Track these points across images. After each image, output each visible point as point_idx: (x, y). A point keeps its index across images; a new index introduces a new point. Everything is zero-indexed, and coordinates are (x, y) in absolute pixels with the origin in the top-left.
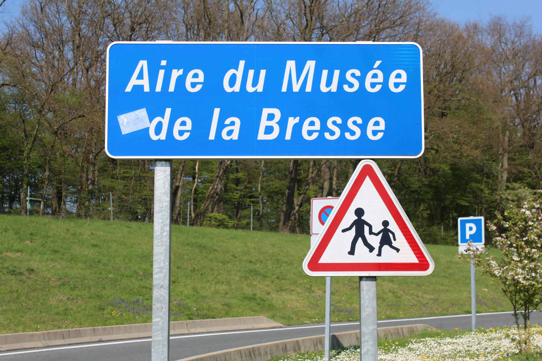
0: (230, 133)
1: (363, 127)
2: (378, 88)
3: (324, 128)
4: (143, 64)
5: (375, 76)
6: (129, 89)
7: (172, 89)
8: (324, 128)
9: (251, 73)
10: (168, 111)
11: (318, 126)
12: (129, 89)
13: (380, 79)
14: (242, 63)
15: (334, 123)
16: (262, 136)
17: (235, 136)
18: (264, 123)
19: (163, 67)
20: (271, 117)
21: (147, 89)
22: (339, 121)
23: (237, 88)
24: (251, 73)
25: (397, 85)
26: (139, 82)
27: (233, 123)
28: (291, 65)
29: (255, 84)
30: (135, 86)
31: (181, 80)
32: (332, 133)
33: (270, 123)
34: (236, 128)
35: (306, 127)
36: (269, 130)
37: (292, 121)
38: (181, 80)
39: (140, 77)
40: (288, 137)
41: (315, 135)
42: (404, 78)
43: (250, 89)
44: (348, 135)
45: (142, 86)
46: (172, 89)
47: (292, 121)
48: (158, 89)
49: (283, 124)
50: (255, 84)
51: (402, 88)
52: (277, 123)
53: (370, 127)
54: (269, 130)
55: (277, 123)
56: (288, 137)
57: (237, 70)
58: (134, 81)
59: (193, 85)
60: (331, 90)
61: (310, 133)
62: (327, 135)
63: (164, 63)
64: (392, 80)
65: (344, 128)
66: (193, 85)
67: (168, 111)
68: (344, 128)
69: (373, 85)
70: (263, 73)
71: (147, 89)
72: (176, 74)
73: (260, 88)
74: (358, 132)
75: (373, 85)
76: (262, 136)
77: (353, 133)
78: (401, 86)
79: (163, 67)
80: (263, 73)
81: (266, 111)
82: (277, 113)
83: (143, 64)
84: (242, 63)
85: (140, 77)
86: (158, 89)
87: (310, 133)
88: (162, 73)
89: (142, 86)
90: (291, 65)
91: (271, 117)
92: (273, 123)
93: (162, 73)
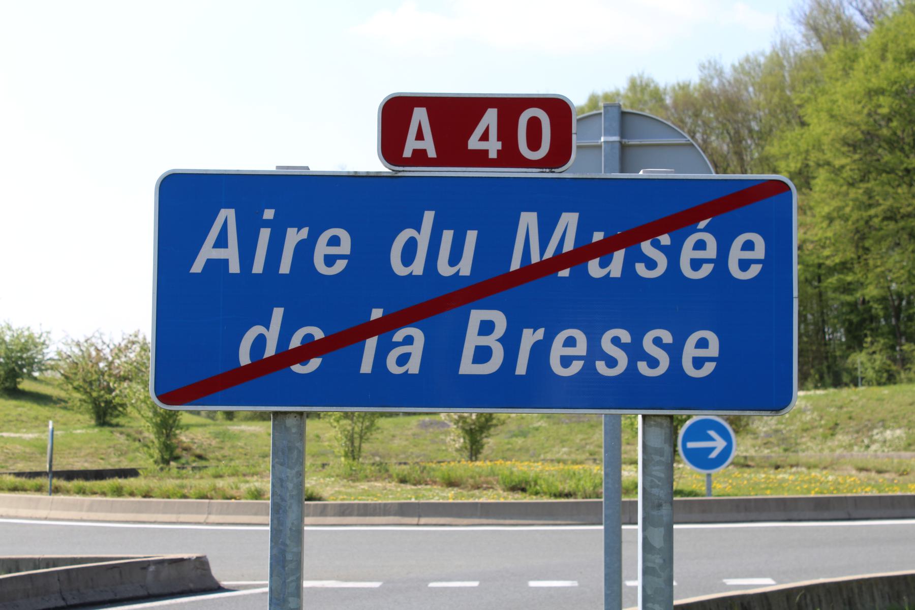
0: (403, 360)
2: (706, 270)
6: (197, 267)
7: (285, 267)
9: (448, 236)
10: (278, 314)
11: (581, 348)
12: (197, 267)
13: (711, 251)
14: (429, 217)
15: (616, 341)
17: (414, 366)
19: (267, 223)
20: (486, 328)
21: (234, 268)
22: (625, 336)
23: (418, 267)
24: (448, 236)
25: (744, 265)
26: (219, 254)
27: (409, 340)
28: (529, 221)
30: (210, 263)
32: (612, 362)
34: (417, 350)
39: (221, 242)
40: (521, 368)
41: (576, 367)
42: (759, 252)
43: (444, 269)
44: (643, 368)
45: (226, 262)
46: (285, 267)
48: (258, 267)
52: (498, 340)
53: (690, 351)
55: (498, 340)
56: (521, 368)
57: (419, 231)
59: (330, 260)
61: (566, 361)
62: (601, 367)
63: (269, 214)
64: (736, 253)
66: (330, 260)
67: (278, 314)
69: (696, 264)
70: (472, 237)
71: (234, 268)
73: (465, 267)
74: (664, 360)
75: (696, 264)
77: (653, 363)
79: (267, 223)
80: (472, 237)
81: (477, 316)
84: (429, 217)
85: (221, 242)
86: (258, 267)
87: (566, 361)
88: (265, 235)
89: (226, 262)
90: (529, 221)
91: (486, 328)
92: (491, 341)
93: (265, 235)
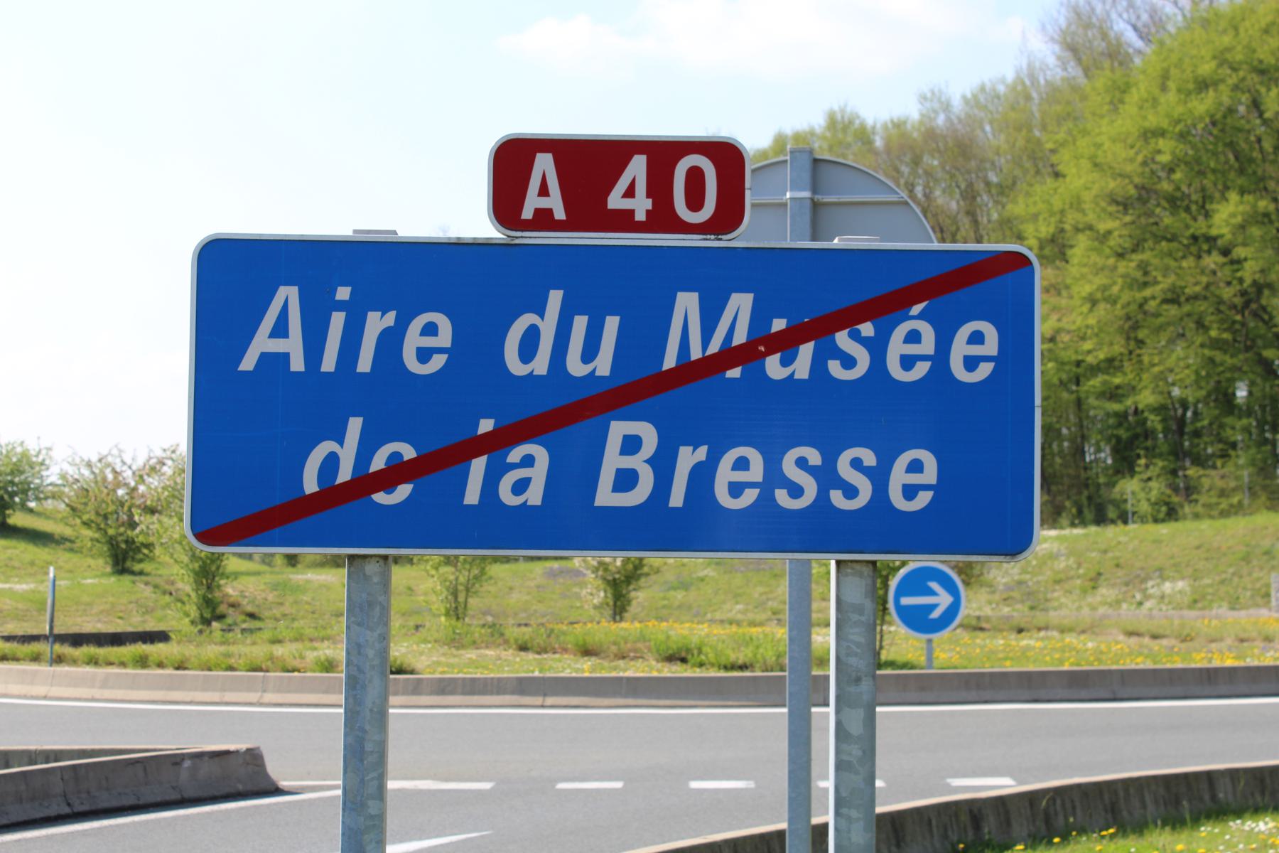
0: (521, 487)
1: (879, 477)
2: (921, 369)
3: (774, 477)
4: (288, 294)
5: (913, 337)
7: (365, 364)
8: (774, 477)
9: (580, 324)
10: (355, 425)
11: (756, 472)
13: (928, 345)
14: (555, 299)
15: (802, 463)
16: (606, 497)
17: (534, 496)
18: (613, 460)
19: (340, 306)
20: (631, 445)
21: (297, 364)
22: (814, 457)
23: (540, 365)
24: (580, 324)
26: (277, 346)
27: (528, 461)
28: (687, 304)
29: (590, 353)
30: (265, 357)
31: (391, 342)
32: (796, 491)
33: (628, 462)
34: (539, 474)
35: (725, 474)
36: (626, 480)
37: (688, 458)
38: (391, 342)
39: (280, 330)
40: (677, 498)
41: (750, 496)
42: (991, 346)
43: (576, 367)
44: (837, 498)
45: (286, 356)
46: (365, 364)
47: (688, 458)
48: (329, 363)
49: (663, 464)
50: (590, 353)
51: (985, 370)
52: (647, 461)
53: (899, 476)
54: (626, 480)
55: (647, 461)
56: (677, 498)
58: (262, 343)
59: (424, 355)
60: (793, 373)
61: (736, 489)
62: (782, 497)
63: (343, 293)
64: (960, 348)
65: (827, 477)
67: (355, 425)
68: (827, 477)
69: (908, 362)
70: (612, 325)
71: (297, 364)
72: (376, 323)
73: (603, 365)
76: (606, 497)
77: (851, 492)
78: (982, 365)
79: (340, 306)
80: (612, 325)
81: (618, 429)
82: (648, 434)
83: (288, 294)
84: (555, 299)
85: (280, 330)
86: (329, 363)
89: (286, 356)
90: (687, 304)
91: (631, 445)
92: (636, 462)
